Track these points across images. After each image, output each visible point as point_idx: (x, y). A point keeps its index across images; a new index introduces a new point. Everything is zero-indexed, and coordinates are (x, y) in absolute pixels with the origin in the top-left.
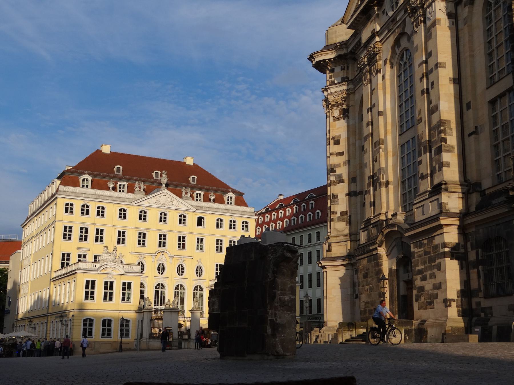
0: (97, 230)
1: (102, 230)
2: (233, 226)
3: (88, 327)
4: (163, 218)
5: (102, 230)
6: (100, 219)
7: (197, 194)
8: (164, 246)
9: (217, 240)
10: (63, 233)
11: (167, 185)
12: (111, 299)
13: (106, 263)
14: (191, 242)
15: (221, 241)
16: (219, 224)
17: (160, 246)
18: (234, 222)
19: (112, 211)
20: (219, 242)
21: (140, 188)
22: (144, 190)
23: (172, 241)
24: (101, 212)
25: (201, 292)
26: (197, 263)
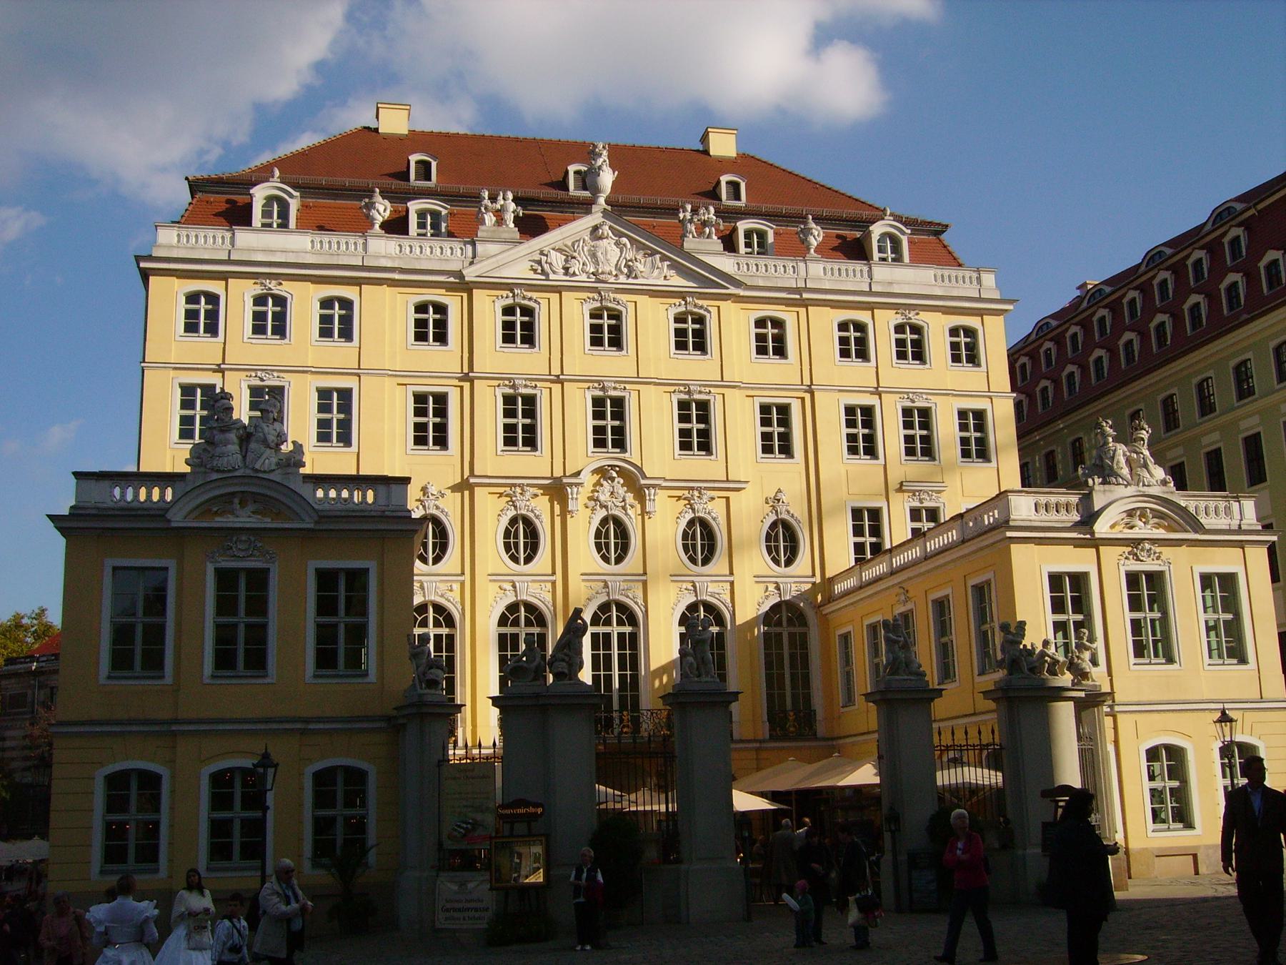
0: (324, 394)
1: (345, 394)
2: (912, 347)
3: (238, 813)
4: (608, 332)
5: (345, 394)
6: (337, 353)
7: (748, 234)
8: (620, 443)
9: (850, 410)
10: (177, 412)
11: (618, 208)
12: (257, 661)
13: (215, 476)
14: (738, 425)
15: (868, 411)
16: (855, 344)
17: (600, 443)
18: (916, 329)
19: (386, 316)
20: (861, 420)
21: (499, 214)
22: (518, 221)
23: (654, 427)
24: (338, 322)
25: (797, 630)
26: (768, 508)
